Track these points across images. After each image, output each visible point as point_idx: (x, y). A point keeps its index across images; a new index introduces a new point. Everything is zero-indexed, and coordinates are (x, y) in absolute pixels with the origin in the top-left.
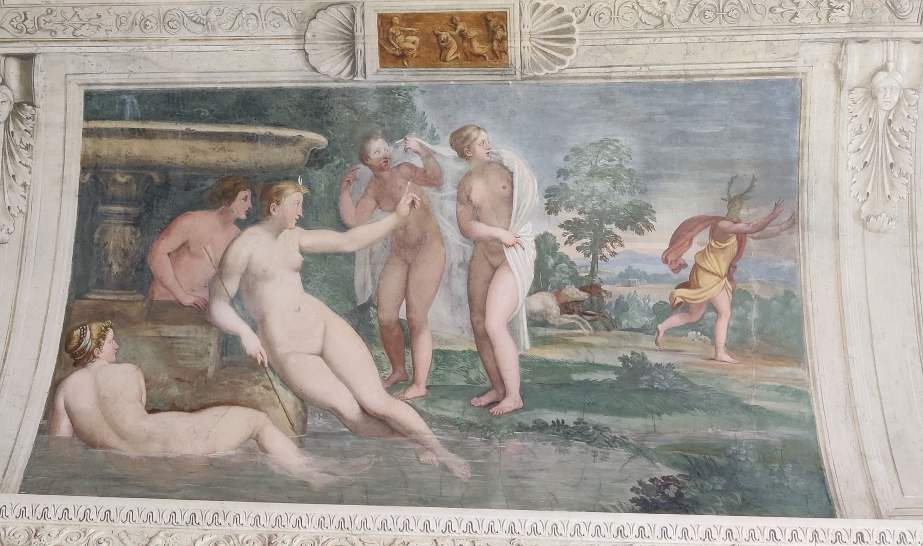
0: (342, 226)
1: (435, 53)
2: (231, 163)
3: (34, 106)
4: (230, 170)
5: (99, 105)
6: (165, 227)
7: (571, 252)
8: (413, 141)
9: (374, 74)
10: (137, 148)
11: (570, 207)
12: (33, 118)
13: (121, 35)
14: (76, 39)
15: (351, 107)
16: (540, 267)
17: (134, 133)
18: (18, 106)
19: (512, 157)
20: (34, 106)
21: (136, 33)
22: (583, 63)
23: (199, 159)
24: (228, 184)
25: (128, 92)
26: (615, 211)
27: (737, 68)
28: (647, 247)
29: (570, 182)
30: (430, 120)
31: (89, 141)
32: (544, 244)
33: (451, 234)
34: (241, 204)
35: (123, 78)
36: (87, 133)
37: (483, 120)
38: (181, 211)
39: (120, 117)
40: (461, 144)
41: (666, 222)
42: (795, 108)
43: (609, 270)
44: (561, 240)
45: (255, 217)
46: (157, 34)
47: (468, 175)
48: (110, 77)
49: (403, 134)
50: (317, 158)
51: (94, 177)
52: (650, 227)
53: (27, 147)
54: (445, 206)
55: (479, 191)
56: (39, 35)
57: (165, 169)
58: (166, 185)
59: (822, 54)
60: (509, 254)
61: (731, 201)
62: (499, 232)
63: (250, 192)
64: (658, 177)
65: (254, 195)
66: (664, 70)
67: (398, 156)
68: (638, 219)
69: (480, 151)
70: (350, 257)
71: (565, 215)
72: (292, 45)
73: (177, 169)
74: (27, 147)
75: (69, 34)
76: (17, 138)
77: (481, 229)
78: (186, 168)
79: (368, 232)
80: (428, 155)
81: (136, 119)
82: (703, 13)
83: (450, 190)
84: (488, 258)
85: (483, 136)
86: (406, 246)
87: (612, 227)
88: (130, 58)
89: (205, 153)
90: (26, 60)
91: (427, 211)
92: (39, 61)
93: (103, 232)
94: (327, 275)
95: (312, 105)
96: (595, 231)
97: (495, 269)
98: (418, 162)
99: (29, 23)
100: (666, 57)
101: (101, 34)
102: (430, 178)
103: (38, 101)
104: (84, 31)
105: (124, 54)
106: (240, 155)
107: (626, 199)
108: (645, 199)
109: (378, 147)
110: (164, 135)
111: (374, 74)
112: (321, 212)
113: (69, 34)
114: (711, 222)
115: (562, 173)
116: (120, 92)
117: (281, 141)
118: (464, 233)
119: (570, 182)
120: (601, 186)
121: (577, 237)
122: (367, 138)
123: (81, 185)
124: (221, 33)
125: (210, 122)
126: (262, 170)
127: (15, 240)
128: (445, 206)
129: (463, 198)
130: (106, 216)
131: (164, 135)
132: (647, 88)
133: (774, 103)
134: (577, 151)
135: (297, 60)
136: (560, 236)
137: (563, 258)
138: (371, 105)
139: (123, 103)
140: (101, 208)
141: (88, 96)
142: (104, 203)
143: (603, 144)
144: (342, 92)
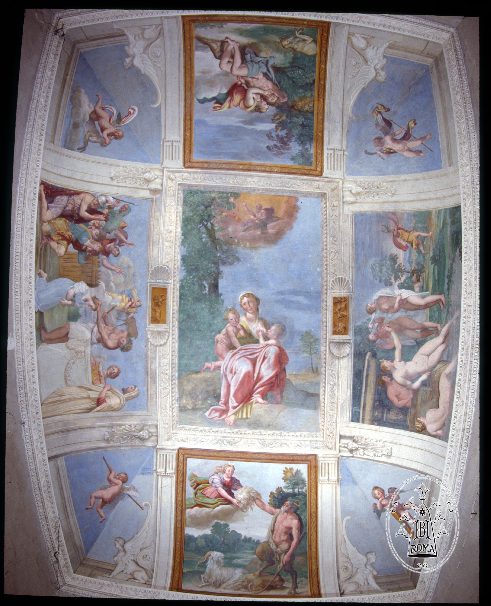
0: (394, 349)
1: (345, 318)
2: (374, 381)
3: (354, 437)
4: (376, 382)
5: (355, 418)
6: (391, 402)
7: (403, 279)
8: (370, 326)
9: (349, 337)
10: (368, 408)
11: (390, 279)
12: (357, 437)
13: (335, 410)
14: (336, 422)
15: (359, 345)
16: (407, 288)
17: (364, 409)
18: (354, 441)
19: (375, 297)
20: (354, 437)
21: (335, 405)
22: (348, 275)
23: (372, 391)
24: (380, 382)
25: (352, 410)
26: (391, 265)
27: (350, 230)
28: (401, 255)
29: (383, 279)
30: (364, 320)
31: (365, 422)
32: (401, 287)
33: (397, 315)
34: (386, 379)
35: (348, 410)
36: (363, 422)
37: (365, 304)
38: (387, 398)
39: (359, 413)
40: (371, 311)
41: (395, 250)
42: (362, 214)
43: (408, 268)
44: (400, 282)
45: (391, 376)
46: (336, 400)
47: (380, 309)
48: (348, 414)
49: (367, 329)
50: (374, 355)
51: (376, 421)
52: (396, 255)
53: (366, 439)
54: (389, 317)
55: (385, 307)
56: (334, 432)
57: (375, 401)
58: (379, 401)
59: (346, 208)
60: (404, 297)
61: (389, 232)
62: (397, 300)
63: (383, 377)
64: (382, 252)
65: (384, 375)
66: (351, 251)
67: (374, 331)
68: (394, 259)
69: (373, 306)
70: (403, 346)
71: (393, 280)
72: (341, 361)
73: (375, 398)
74: (366, 439)
75: (335, 424)
76: (363, 442)
77: (396, 305)
78: (375, 395)
79: (396, 341)
80: (374, 322)
81: (360, 408)
82: (335, 241)
83: (385, 315)
84: (404, 304)
85: (369, 305)
86: (400, 330)
87: (396, 266)
88: (342, 407)
89: (371, 389)
90: (341, 437)
91: (390, 323)
92: (342, 434)
93: (391, 420)
94: (408, 354)
95: (359, 355)
96: (397, 271)
97: (407, 302)
98: (376, 325)
99: (331, 435)
100: (347, 252)
101: (335, 415)
102: (381, 321)
103: (353, 435)
104: (334, 420)
105: (341, 409)
106: (372, 379)
107: (388, 262)
108: (388, 256)
109: (371, 337)
110: (365, 400)
111: (349, 337)
112: (390, 354)
113: (335, 424)
114: (395, 237)
115: (380, 281)
116: (352, 412)
117: (369, 366)
118: (397, 311)
119: (383, 279)
120: (384, 269)
121: (399, 277)
122: (369, 340)
123: (377, 425)
124: (336, 381)
125: (362, 387)
126: (377, 372)
127: (391, 445)
128: (389, 317)
129: (387, 311)
130: (386, 419)
131: (365, 400)
132: (356, 257)
133: (360, 219)
134: (374, 277)
135: (345, 360)
136: (398, 282)
137: (405, 281)
138: (359, 338)
139: (355, 411)
140: (384, 420)
141: (352, 421)
142: (383, 419)
143: (373, 269)
144: (355, 346)
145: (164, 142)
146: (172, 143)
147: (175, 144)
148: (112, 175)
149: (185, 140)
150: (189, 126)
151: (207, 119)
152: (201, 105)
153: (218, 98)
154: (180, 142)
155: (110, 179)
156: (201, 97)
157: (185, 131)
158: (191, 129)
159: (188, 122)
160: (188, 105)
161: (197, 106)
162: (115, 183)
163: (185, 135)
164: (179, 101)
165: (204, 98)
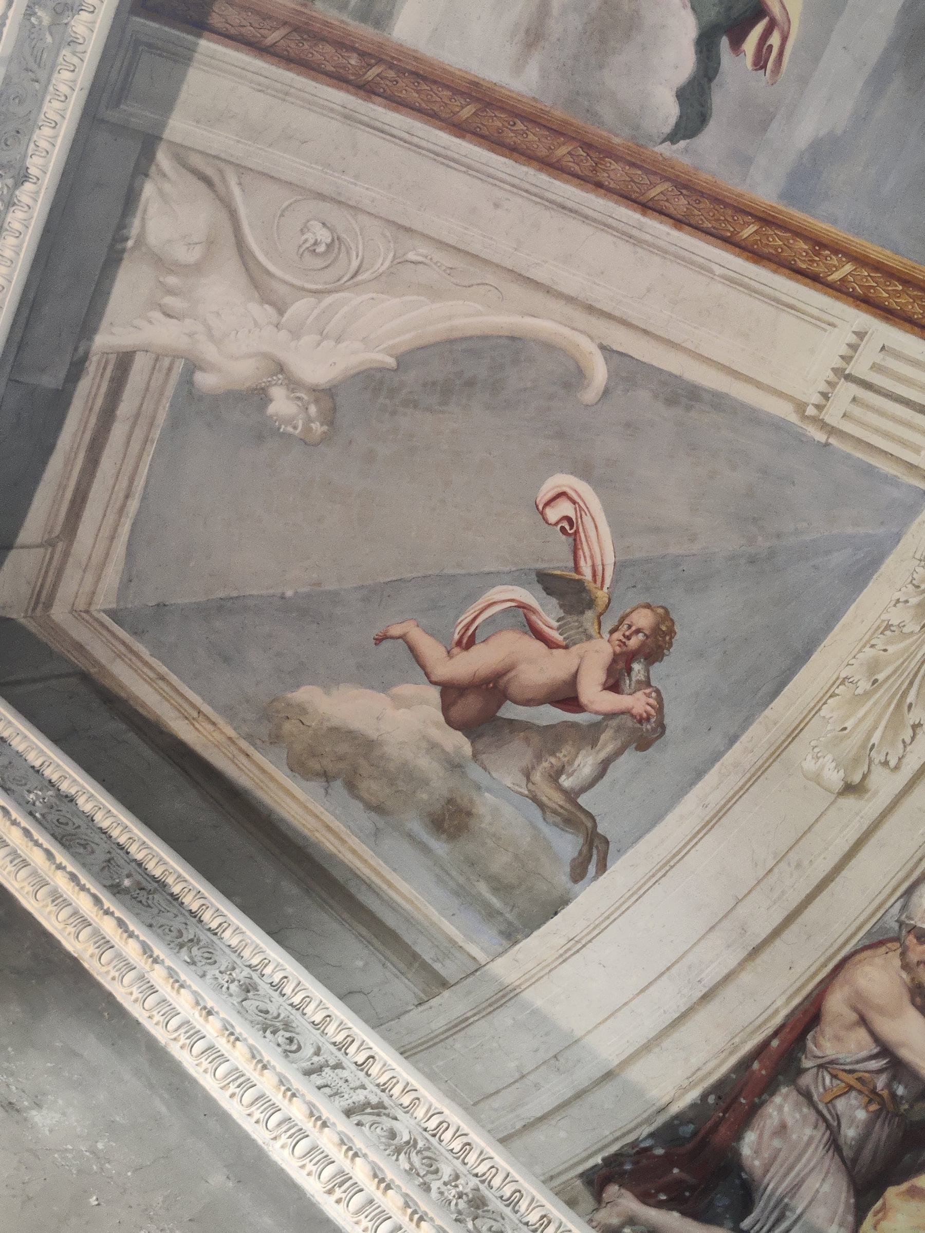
145: (814, 420)
146: (849, 378)
147: (860, 368)
148: (835, 778)
149: (866, 302)
150: (802, 245)
151: (807, 127)
152: (712, 126)
153: (713, 13)
154: (861, 335)
155: (849, 802)
156: (667, 110)
157: (814, 279)
158: (819, 244)
159: (775, 240)
160: (680, 205)
161: (707, 156)
162: (885, 786)
163: (839, 290)
164: (638, 242)
165: (681, 95)
